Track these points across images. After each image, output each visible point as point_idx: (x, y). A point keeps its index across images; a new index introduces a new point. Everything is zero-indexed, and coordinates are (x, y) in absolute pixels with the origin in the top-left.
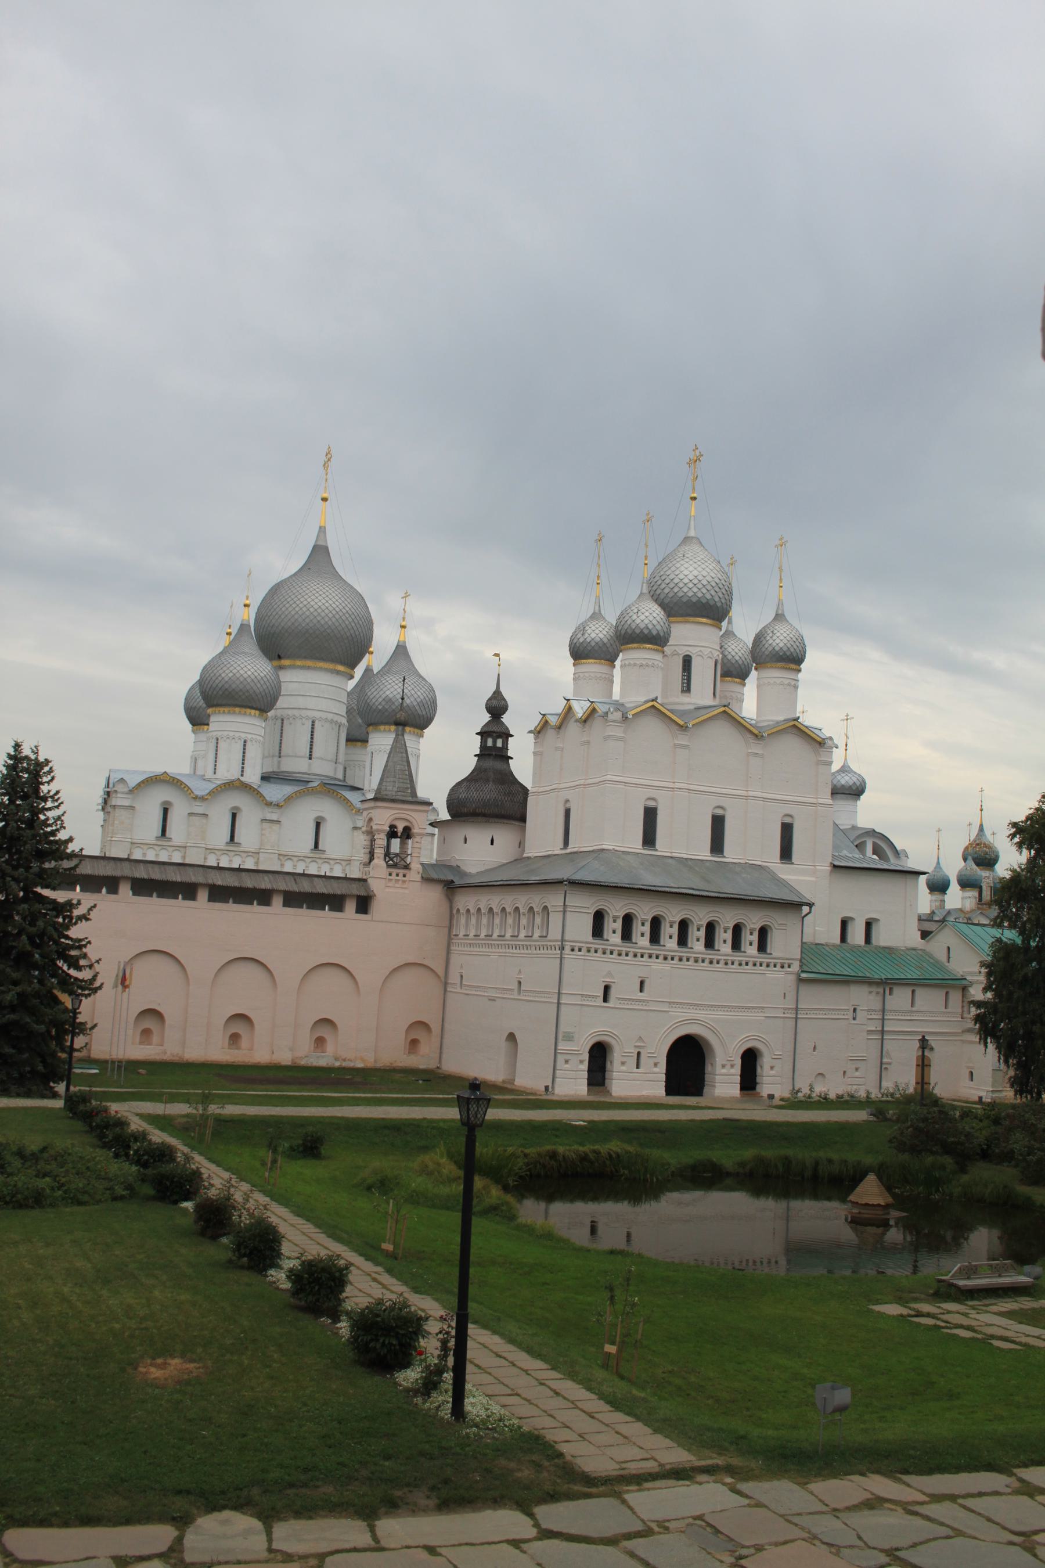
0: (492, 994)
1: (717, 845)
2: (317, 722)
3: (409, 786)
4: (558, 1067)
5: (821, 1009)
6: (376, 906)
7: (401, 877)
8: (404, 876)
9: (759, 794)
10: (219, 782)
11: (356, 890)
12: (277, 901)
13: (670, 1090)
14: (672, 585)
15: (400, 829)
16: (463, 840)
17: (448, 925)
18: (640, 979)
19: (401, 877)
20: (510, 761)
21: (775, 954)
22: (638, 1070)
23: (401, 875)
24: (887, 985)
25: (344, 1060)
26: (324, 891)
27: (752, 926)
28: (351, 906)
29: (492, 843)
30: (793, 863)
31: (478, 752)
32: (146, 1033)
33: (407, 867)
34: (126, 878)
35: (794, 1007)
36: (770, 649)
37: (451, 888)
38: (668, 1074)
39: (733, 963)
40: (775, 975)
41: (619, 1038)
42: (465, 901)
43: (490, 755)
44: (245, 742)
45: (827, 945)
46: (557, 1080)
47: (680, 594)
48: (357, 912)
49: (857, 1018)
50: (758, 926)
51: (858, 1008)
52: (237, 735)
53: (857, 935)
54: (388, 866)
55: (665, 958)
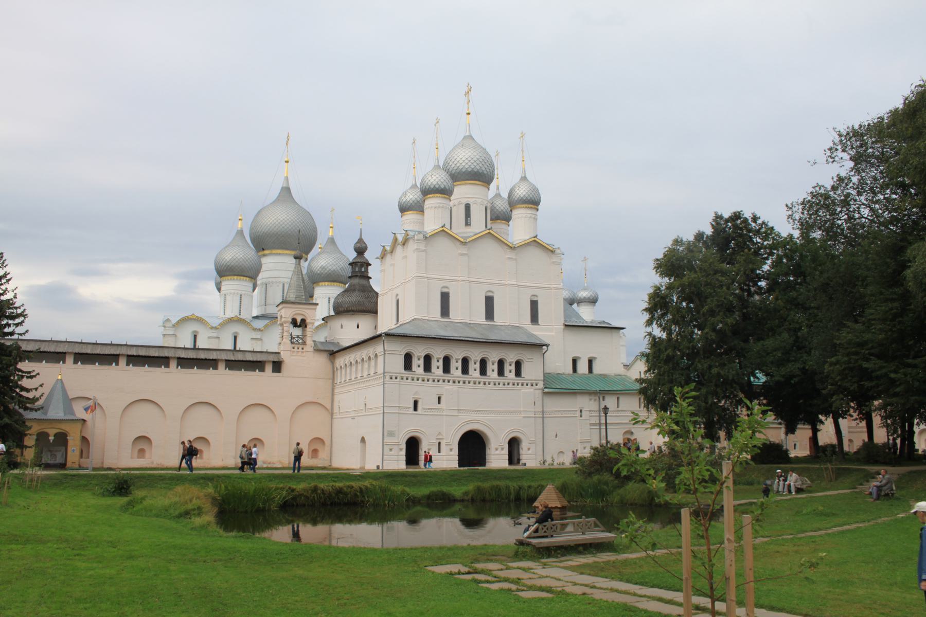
0: (353, 414)
1: (490, 313)
3: (303, 294)
4: (385, 453)
5: (559, 411)
6: (284, 368)
9: (515, 283)
11: (272, 358)
13: (460, 466)
14: (456, 162)
15: (299, 321)
16: (340, 327)
17: (332, 377)
20: (370, 280)
23: (300, 348)
24: (601, 394)
25: (270, 463)
26: (252, 359)
27: (510, 360)
28: (269, 368)
29: (358, 327)
30: (539, 325)
31: (350, 275)
33: (304, 343)
34: (123, 355)
35: (541, 410)
36: (518, 196)
37: (333, 354)
38: (459, 455)
39: (499, 384)
40: (528, 390)
42: (341, 361)
43: (357, 276)
44: (241, 295)
45: (564, 374)
46: (385, 462)
47: (461, 167)
49: (583, 417)
50: (514, 360)
52: (236, 292)
53: (583, 368)
54: (292, 343)
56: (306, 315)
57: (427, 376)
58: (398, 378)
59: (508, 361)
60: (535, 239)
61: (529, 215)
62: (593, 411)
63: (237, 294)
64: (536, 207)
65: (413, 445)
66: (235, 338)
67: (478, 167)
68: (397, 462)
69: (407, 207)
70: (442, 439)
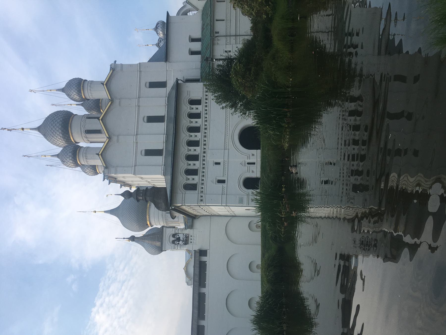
3: (156, 236)
7: (192, 238)
8: (191, 236)
11: (198, 255)
12: (203, 290)
15: (174, 239)
17: (210, 217)
18: (214, 165)
19: (192, 238)
21: (201, 96)
22: (256, 164)
27: (189, 108)
28: (204, 259)
41: (240, 175)
48: (207, 256)
49: (230, 50)
50: (189, 106)
51: (225, 50)
53: (197, 46)
56: (170, 234)
57: (200, 173)
58: (201, 195)
59: (190, 111)
60: (105, 84)
61: (89, 88)
62: (226, 42)
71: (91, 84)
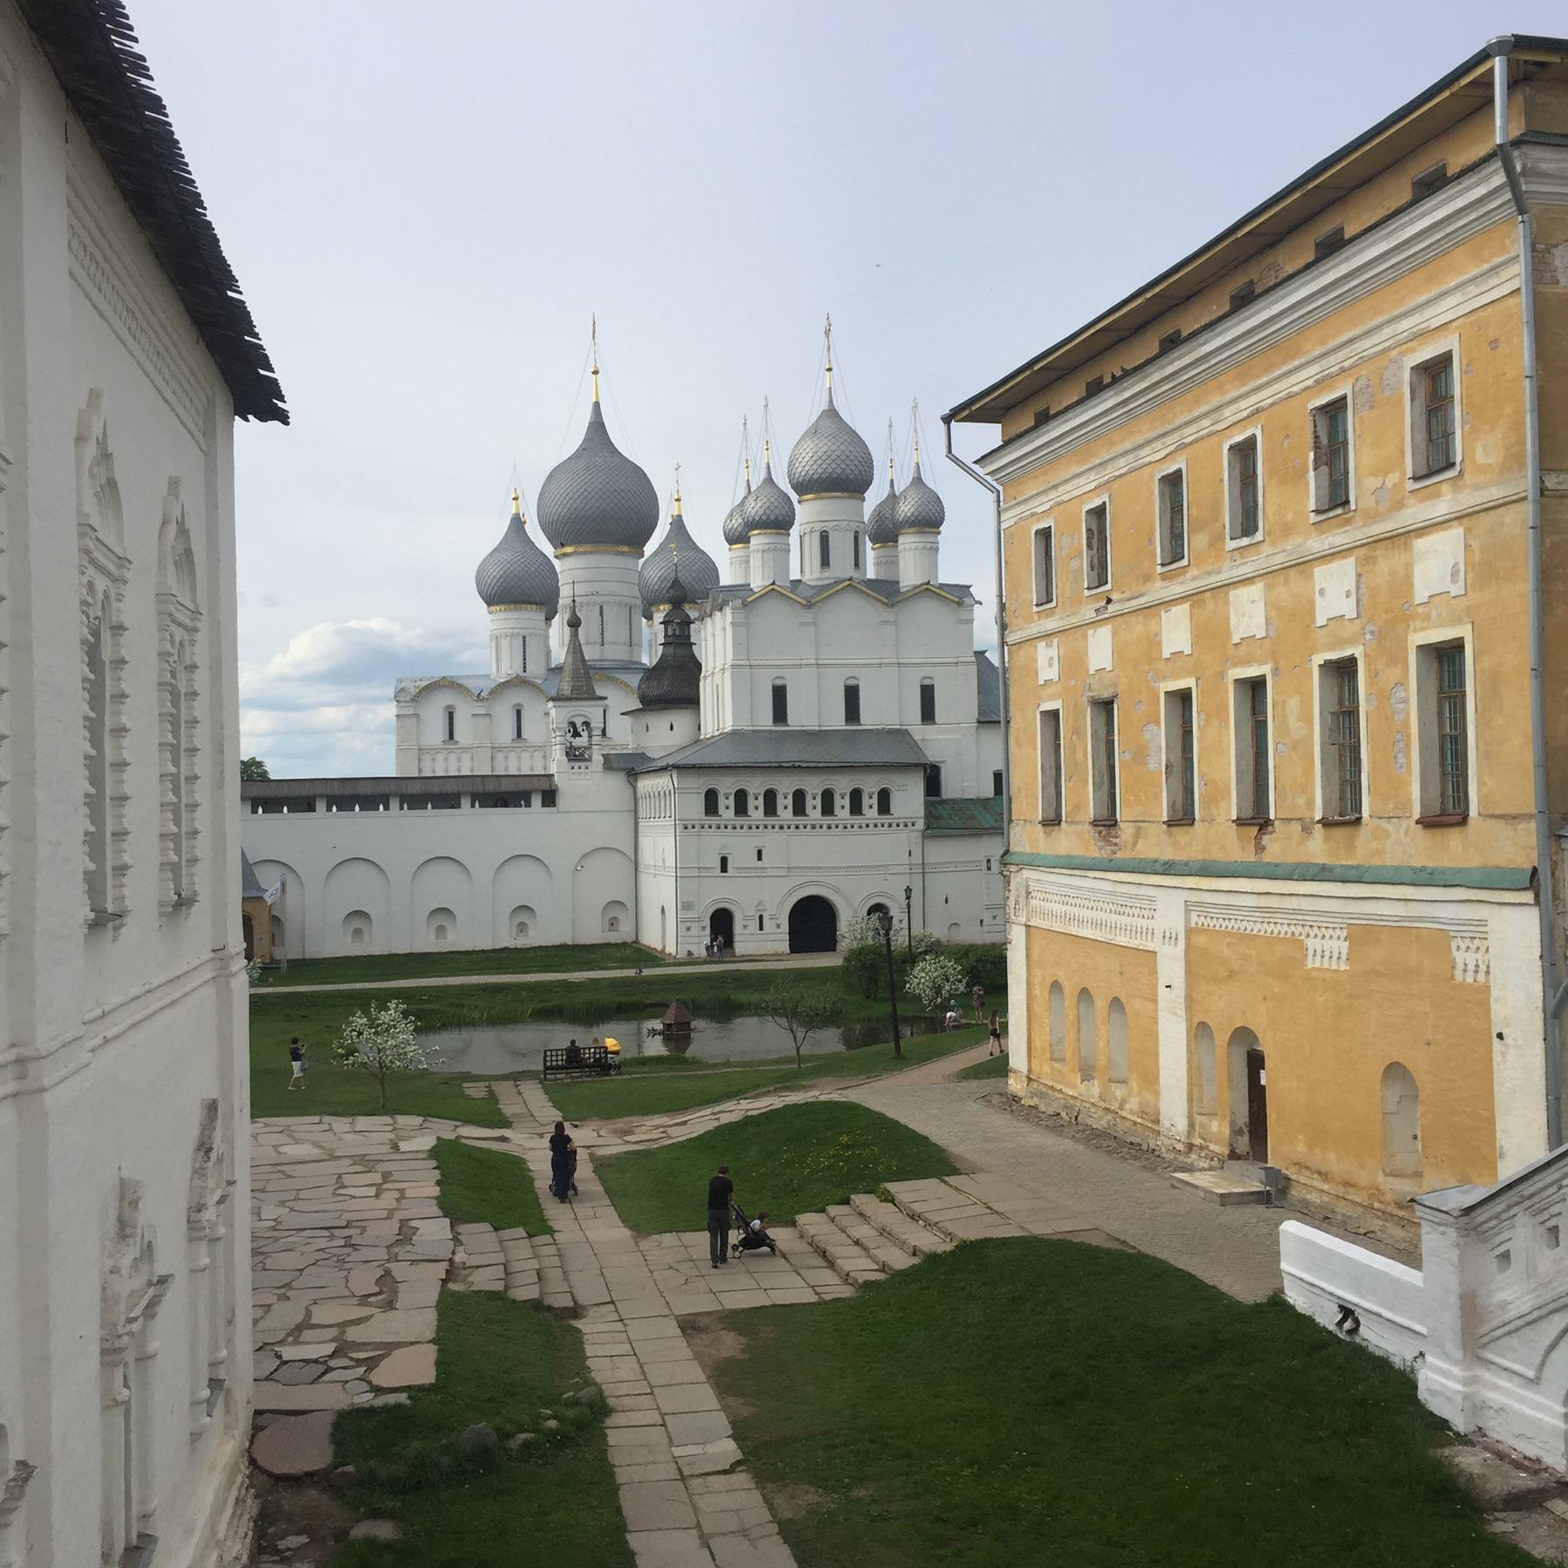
1: (852, 712)
2: (605, 607)
7: (583, 770)
10: (502, 680)
12: (465, 802)
21: (896, 815)
27: (871, 790)
28: (536, 800)
29: (672, 729)
30: (935, 724)
32: (358, 932)
33: (589, 760)
34: (321, 796)
36: (903, 515)
42: (646, 784)
44: (524, 637)
50: (876, 790)
55: (781, 827)
63: (518, 634)
64: (935, 530)
65: (722, 922)
66: (519, 713)
67: (839, 471)
68: (700, 941)
69: (735, 538)
70: (764, 910)
71: (931, 549)
